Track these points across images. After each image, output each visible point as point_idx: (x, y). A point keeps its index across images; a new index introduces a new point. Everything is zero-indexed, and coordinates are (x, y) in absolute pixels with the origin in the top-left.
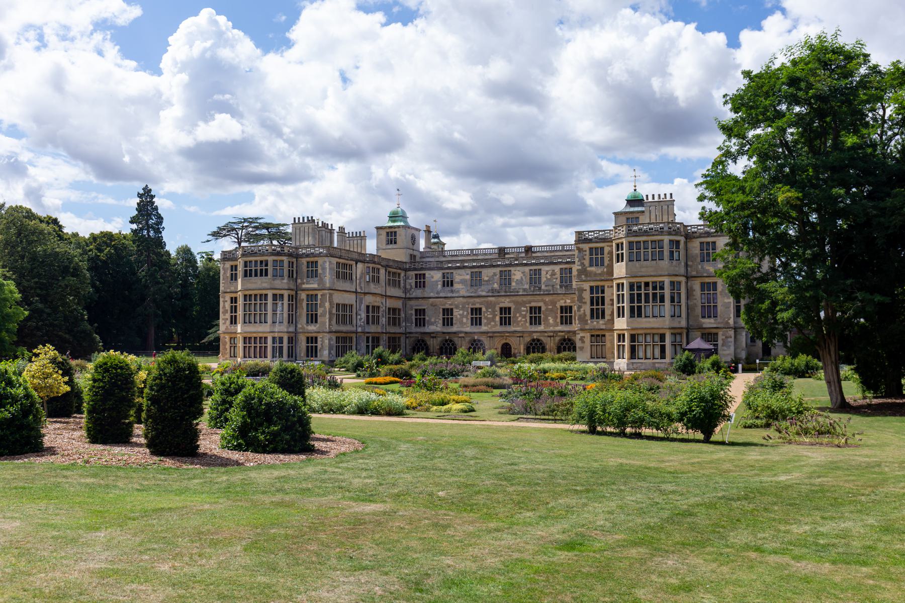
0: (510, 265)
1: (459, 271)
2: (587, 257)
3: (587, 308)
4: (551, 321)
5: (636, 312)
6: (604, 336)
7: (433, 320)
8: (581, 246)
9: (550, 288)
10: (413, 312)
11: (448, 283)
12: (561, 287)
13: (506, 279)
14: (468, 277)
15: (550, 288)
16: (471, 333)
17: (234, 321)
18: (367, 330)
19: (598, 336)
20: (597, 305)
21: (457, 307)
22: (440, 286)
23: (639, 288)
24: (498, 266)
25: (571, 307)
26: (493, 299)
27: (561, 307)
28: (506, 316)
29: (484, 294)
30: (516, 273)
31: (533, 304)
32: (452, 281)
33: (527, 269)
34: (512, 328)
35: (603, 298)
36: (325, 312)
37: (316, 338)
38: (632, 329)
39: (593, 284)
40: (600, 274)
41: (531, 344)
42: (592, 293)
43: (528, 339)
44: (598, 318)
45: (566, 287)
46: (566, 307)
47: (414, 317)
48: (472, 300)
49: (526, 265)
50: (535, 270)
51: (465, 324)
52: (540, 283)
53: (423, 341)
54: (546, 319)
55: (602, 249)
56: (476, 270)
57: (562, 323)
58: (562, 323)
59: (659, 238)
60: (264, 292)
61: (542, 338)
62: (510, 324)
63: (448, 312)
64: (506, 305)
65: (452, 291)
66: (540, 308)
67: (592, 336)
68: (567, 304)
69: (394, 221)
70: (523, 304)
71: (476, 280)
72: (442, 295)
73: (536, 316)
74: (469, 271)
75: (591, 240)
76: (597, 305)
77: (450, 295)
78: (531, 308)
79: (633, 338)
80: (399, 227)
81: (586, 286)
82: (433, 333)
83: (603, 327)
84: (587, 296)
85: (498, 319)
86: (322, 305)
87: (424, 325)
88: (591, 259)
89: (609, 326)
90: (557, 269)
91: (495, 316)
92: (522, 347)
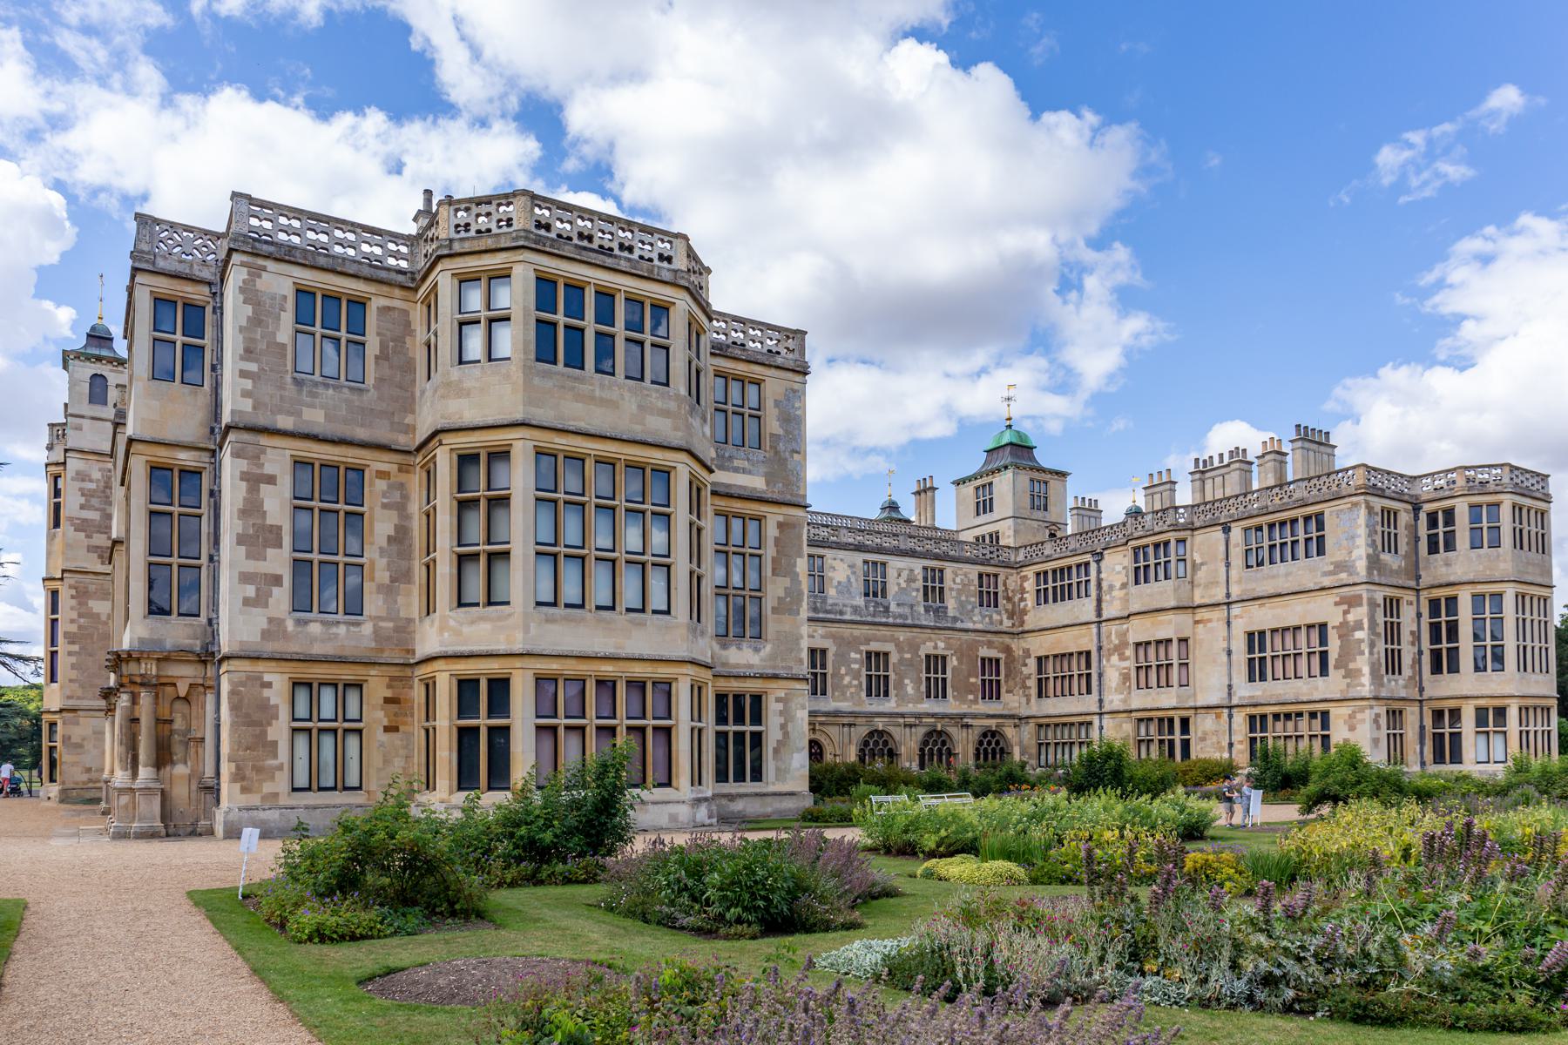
4: (910, 690)
9: (907, 610)
12: (927, 610)
15: (907, 610)
25: (944, 658)
27: (928, 657)
30: (836, 564)
31: (875, 646)
33: (859, 558)
36: (793, 595)
37: (757, 699)
40: (1397, 573)
43: (862, 731)
45: (936, 611)
46: (936, 657)
49: (859, 548)
50: (875, 563)
52: (884, 595)
54: (900, 685)
57: (929, 696)
61: (891, 729)
62: (824, 693)
66: (886, 654)
68: (939, 652)
78: (869, 654)
86: (782, 567)
90: (918, 565)
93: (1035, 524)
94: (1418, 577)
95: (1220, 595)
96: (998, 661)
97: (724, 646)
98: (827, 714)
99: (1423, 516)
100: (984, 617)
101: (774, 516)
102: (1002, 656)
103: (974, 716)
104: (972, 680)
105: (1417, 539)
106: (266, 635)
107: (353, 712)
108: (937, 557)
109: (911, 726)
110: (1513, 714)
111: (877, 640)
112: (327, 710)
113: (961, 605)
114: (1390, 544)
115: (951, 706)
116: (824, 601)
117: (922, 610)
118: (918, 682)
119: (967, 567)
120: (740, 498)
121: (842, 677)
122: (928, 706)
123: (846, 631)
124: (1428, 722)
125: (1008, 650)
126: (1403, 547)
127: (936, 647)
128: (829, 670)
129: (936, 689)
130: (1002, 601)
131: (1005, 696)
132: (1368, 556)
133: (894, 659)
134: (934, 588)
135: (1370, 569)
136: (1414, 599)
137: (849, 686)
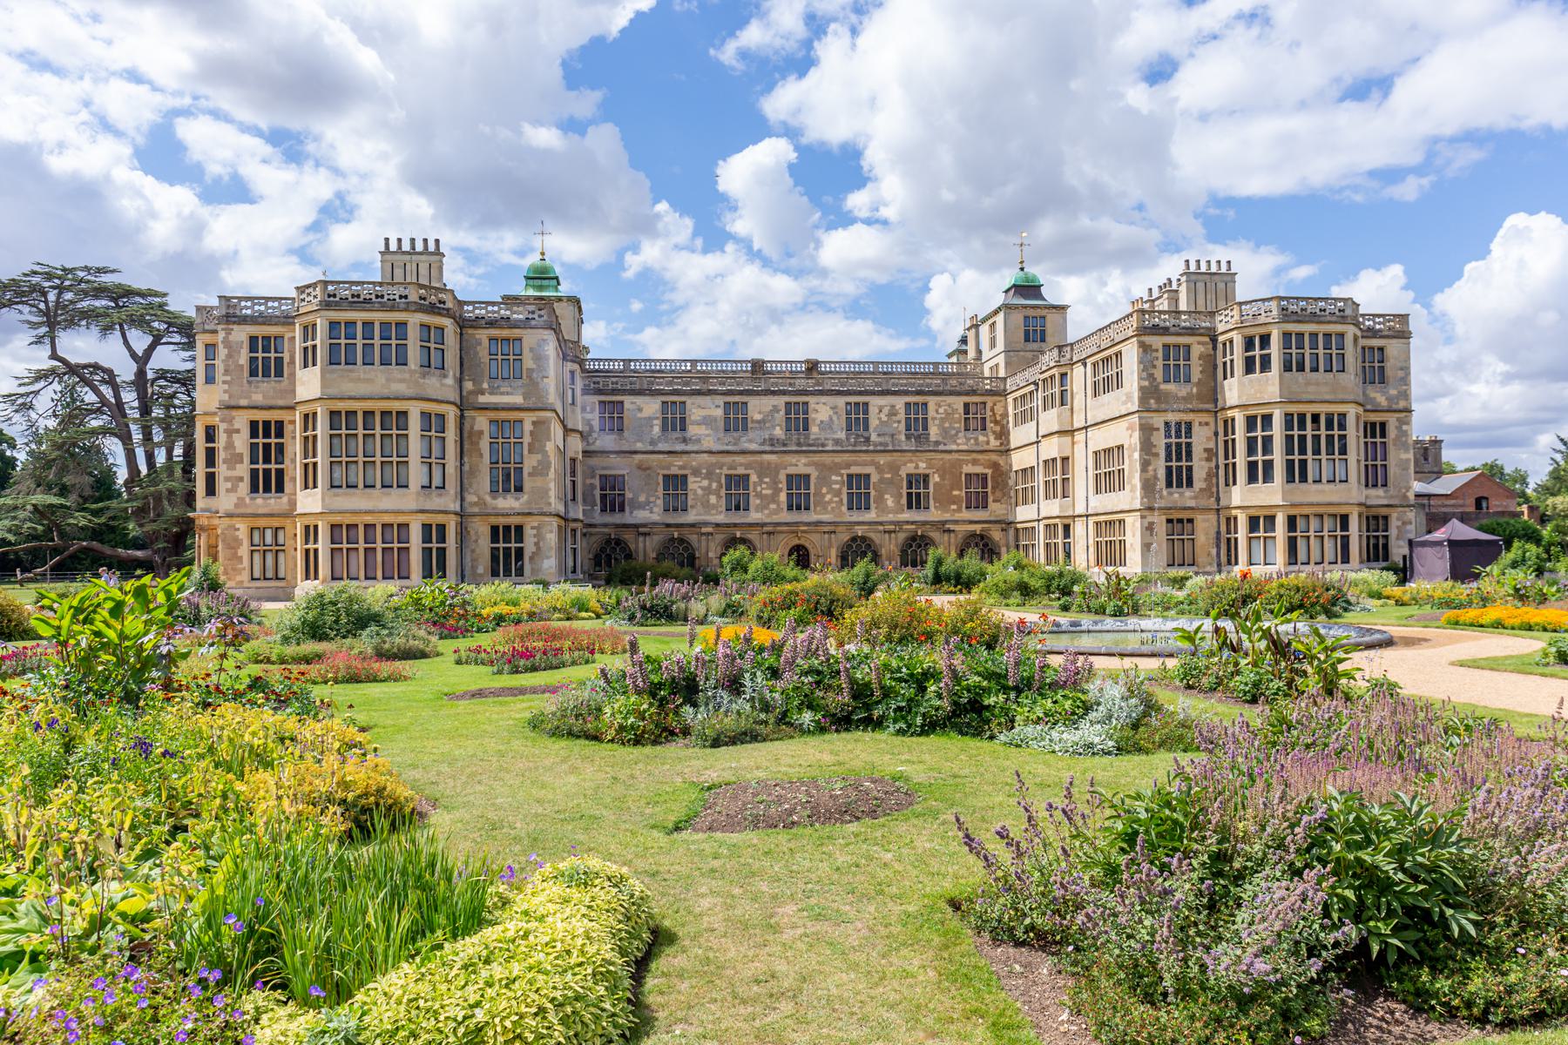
0: (804, 393)
1: (700, 400)
2: (1160, 363)
3: (1160, 466)
4: (890, 502)
5: (1297, 473)
6: (1190, 521)
7: (642, 498)
8: (1148, 339)
9: (888, 439)
10: (597, 482)
11: (675, 421)
12: (908, 437)
13: (798, 420)
14: (719, 412)
15: (888, 439)
16: (728, 525)
17: (268, 481)
18: (572, 515)
19: (1180, 521)
20: (1179, 459)
21: (696, 472)
22: (657, 429)
23: (1302, 426)
24: (784, 393)
26: (773, 457)
28: (799, 493)
29: (754, 447)
31: (855, 470)
32: (683, 420)
33: (841, 401)
34: (812, 516)
35: (1189, 445)
38: (1292, 505)
39: (1172, 417)
40: (1184, 398)
41: (849, 547)
42: (1168, 436)
43: (846, 537)
44: (1180, 485)
47: (597, 493)
48: (728, 459)
49: (839, 393)
51: (714, 507)
52: (866, 428)
53: (618, 542)
54: (880, 500)
55: (1188, 347)
56: (737, 399)
57: (910, 506)
58: (910, 506)
59: (1339, 328)
60: (397, 406)
61: (872, 535)
62: (807, 508)
63: (676, 484)
64: (802, 470)
65: (685, 440)
67: (1169, 521)
69: (541, 288)
70: (835, 468)
71: (735, 421)
72: (661, 447)
73: (859, 492)
74: (720, 400)
75: (1166, 329)
76: (1179, 459)
77: (679, 447)
79: (1292, 522)
80: (560, 299)
81: (1158, 421)
82: (644, 525)
83: (1192, 503)
84: (1160, 441)
85: (783, 497)
87: (622, 510)
88: (1167, 367)
89: (1203, 503)
90: (899, 402)
91: (777, 491)
92: (834, 552)
93: (1029, 355)
94: (1216, 401)
95: (1083, 424)
96: (984, 477)
97: (494, 498)
98: (808, 524)
99: (1220, 346)
100: (968, 439)
101: (528, 419)
102: (989, 471)
103: (956, 522)
104: (956, 493)
105: (1215, 367)
106: (236, 505)
107: (281, 541)
108: (919, 393)
109: (890, 532)
110: (1280, 520)
111: (856, 464)
112: (269, 540)
113: (945, 432)
114: (1175, 373)
115: (934, 514)
116: (807, 437)
117: (903, 438)
118: (898, 496)
119: (950, 399)
120: (496, 409)
121: (824, 496)
122: (907, 516)
123: (827, 459)
124: (1223, 528)
125: (995, 466)
126: (1196, 375)
127: (917, 467)
128: (812, 491)
129: (915, 502)
130: (990, 425)
131: (992, 506)
132: (1141, 388)
133: (874, 479)
134: (916, 420)
135: (1143, 399)
136: (1211, 420)
137: (831, 501)
